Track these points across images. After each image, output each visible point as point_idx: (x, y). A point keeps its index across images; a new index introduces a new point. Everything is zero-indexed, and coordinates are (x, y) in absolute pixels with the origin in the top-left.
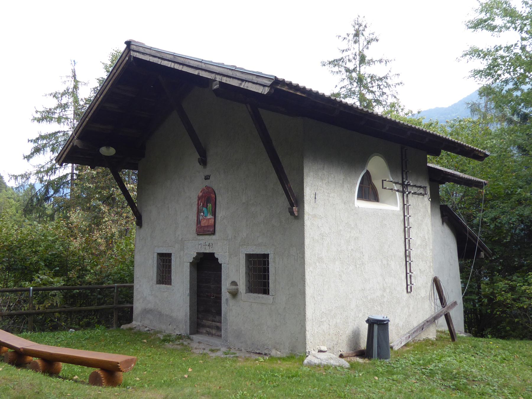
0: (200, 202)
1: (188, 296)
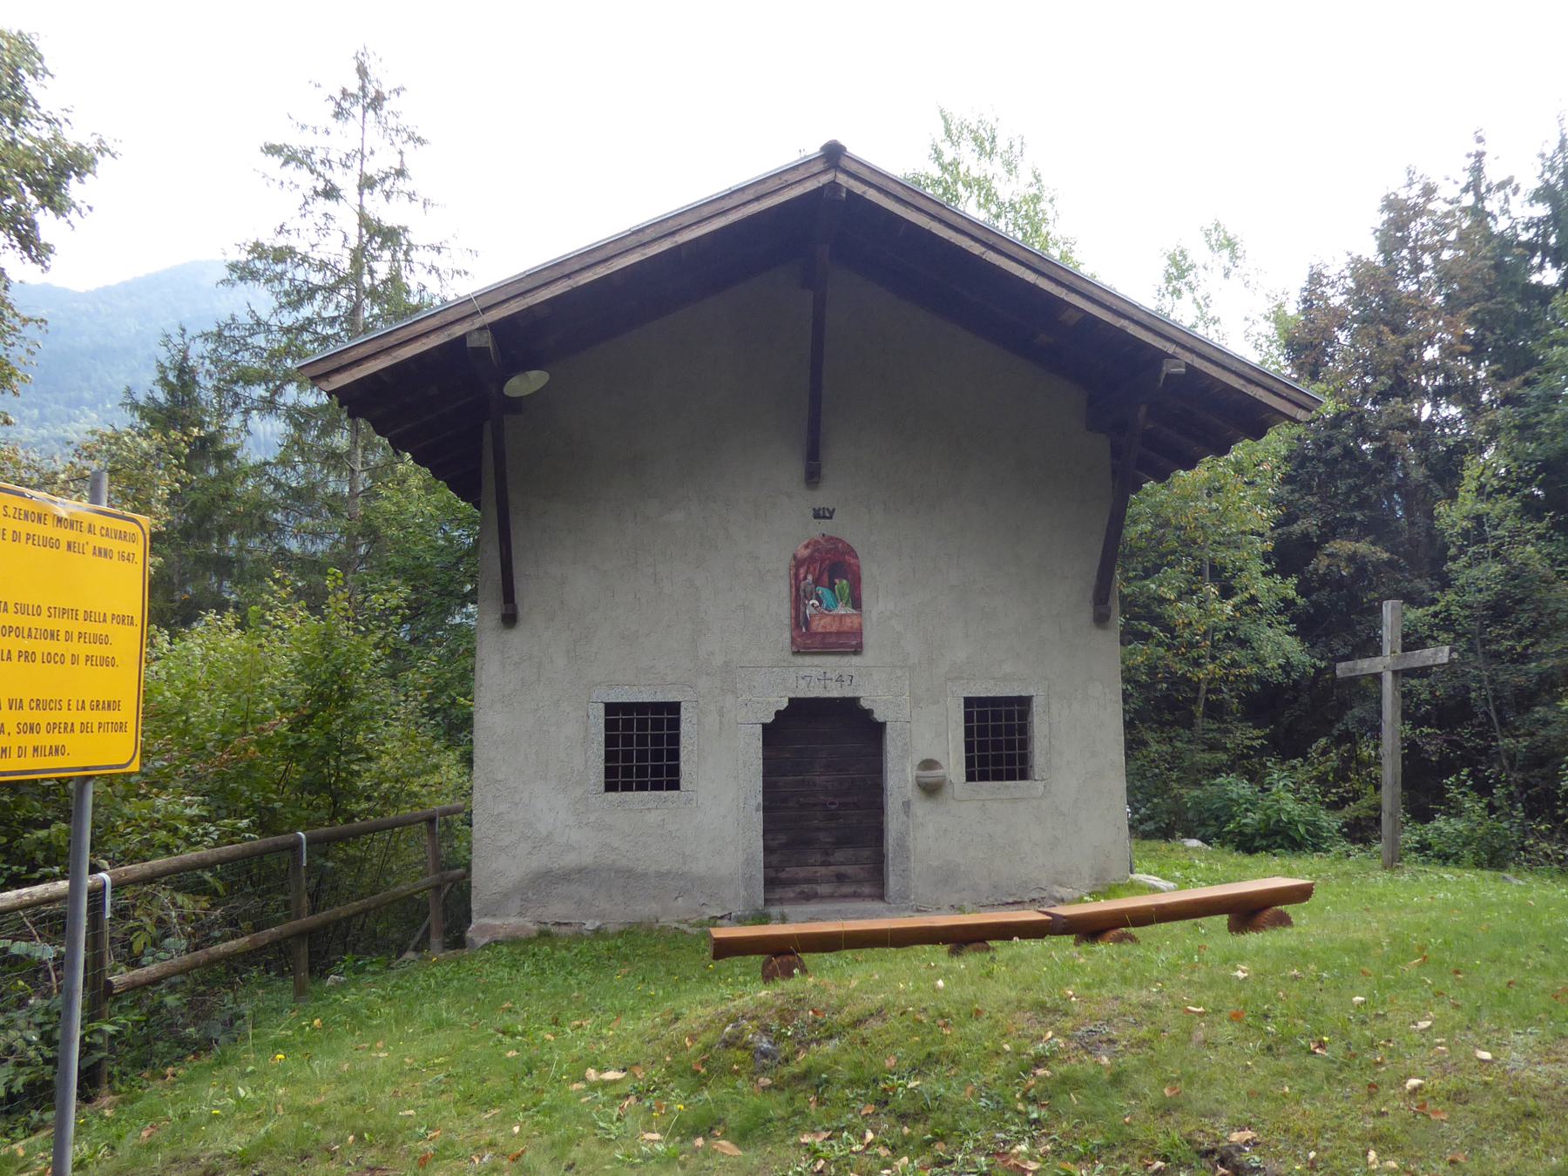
0: (802, 571)
1: (757, 810)
